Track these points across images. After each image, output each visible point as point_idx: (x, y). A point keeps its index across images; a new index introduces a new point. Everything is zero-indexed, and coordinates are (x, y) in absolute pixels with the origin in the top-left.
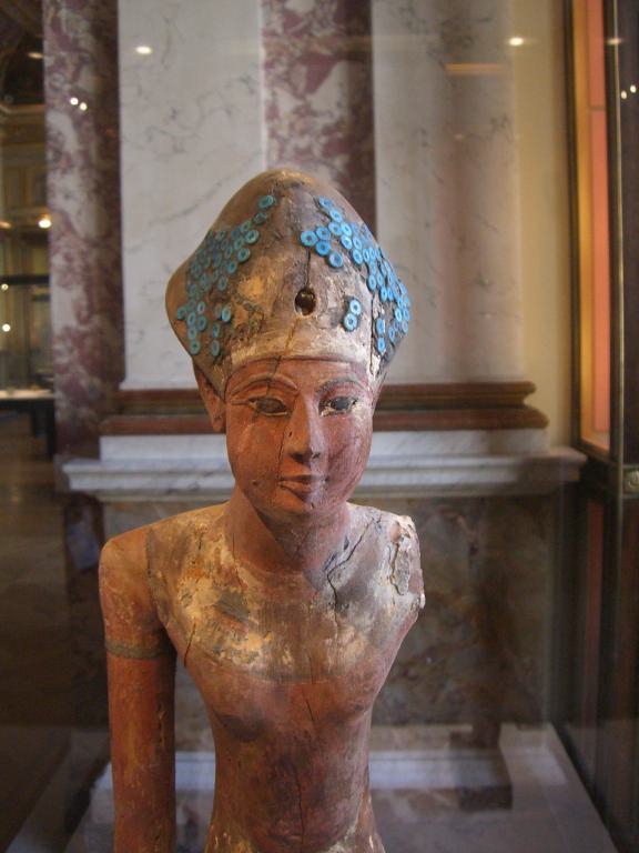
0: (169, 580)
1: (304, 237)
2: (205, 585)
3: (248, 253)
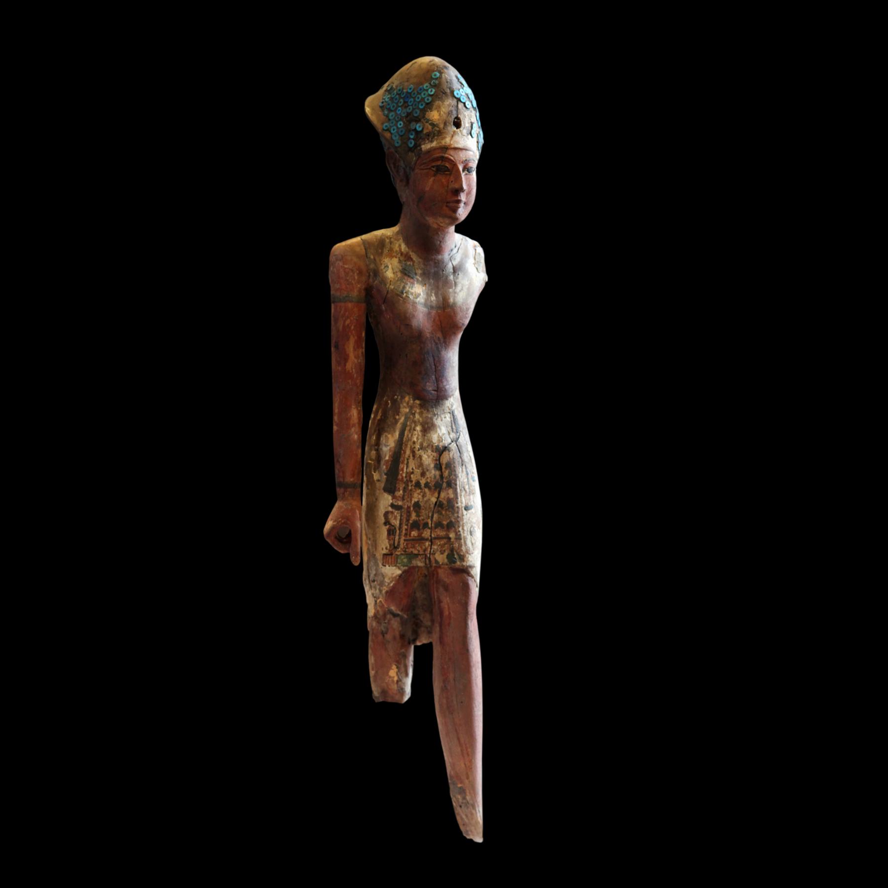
0: (377, 259)
1: (455, 93)
2: (395, 261)
3: (430, 99)
